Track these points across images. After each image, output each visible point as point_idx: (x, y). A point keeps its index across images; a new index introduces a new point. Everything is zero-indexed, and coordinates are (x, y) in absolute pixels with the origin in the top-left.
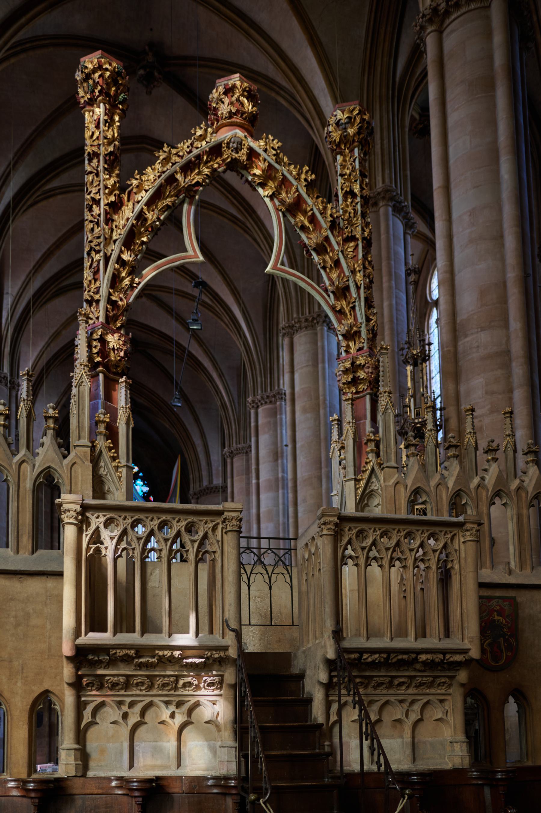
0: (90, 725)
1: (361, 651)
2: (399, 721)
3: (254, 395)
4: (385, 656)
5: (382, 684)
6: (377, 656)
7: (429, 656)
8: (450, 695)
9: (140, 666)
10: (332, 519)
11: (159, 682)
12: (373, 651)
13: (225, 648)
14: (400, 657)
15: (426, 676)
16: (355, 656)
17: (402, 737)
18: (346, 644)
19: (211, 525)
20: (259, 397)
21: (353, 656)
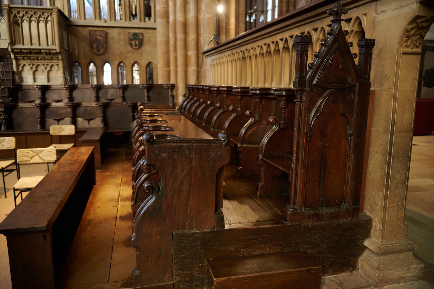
1: (21, 49)
2: (43, 70)
6: (26, 50)
7: (44, 51)
8: (59, 63)
10: (6, 8)
12: (25, 49)
14: (34, 51)
15: (49, 57)
16: (20, 50)
17: (45, 75)
18: (15, 47)
21: (18, 50)
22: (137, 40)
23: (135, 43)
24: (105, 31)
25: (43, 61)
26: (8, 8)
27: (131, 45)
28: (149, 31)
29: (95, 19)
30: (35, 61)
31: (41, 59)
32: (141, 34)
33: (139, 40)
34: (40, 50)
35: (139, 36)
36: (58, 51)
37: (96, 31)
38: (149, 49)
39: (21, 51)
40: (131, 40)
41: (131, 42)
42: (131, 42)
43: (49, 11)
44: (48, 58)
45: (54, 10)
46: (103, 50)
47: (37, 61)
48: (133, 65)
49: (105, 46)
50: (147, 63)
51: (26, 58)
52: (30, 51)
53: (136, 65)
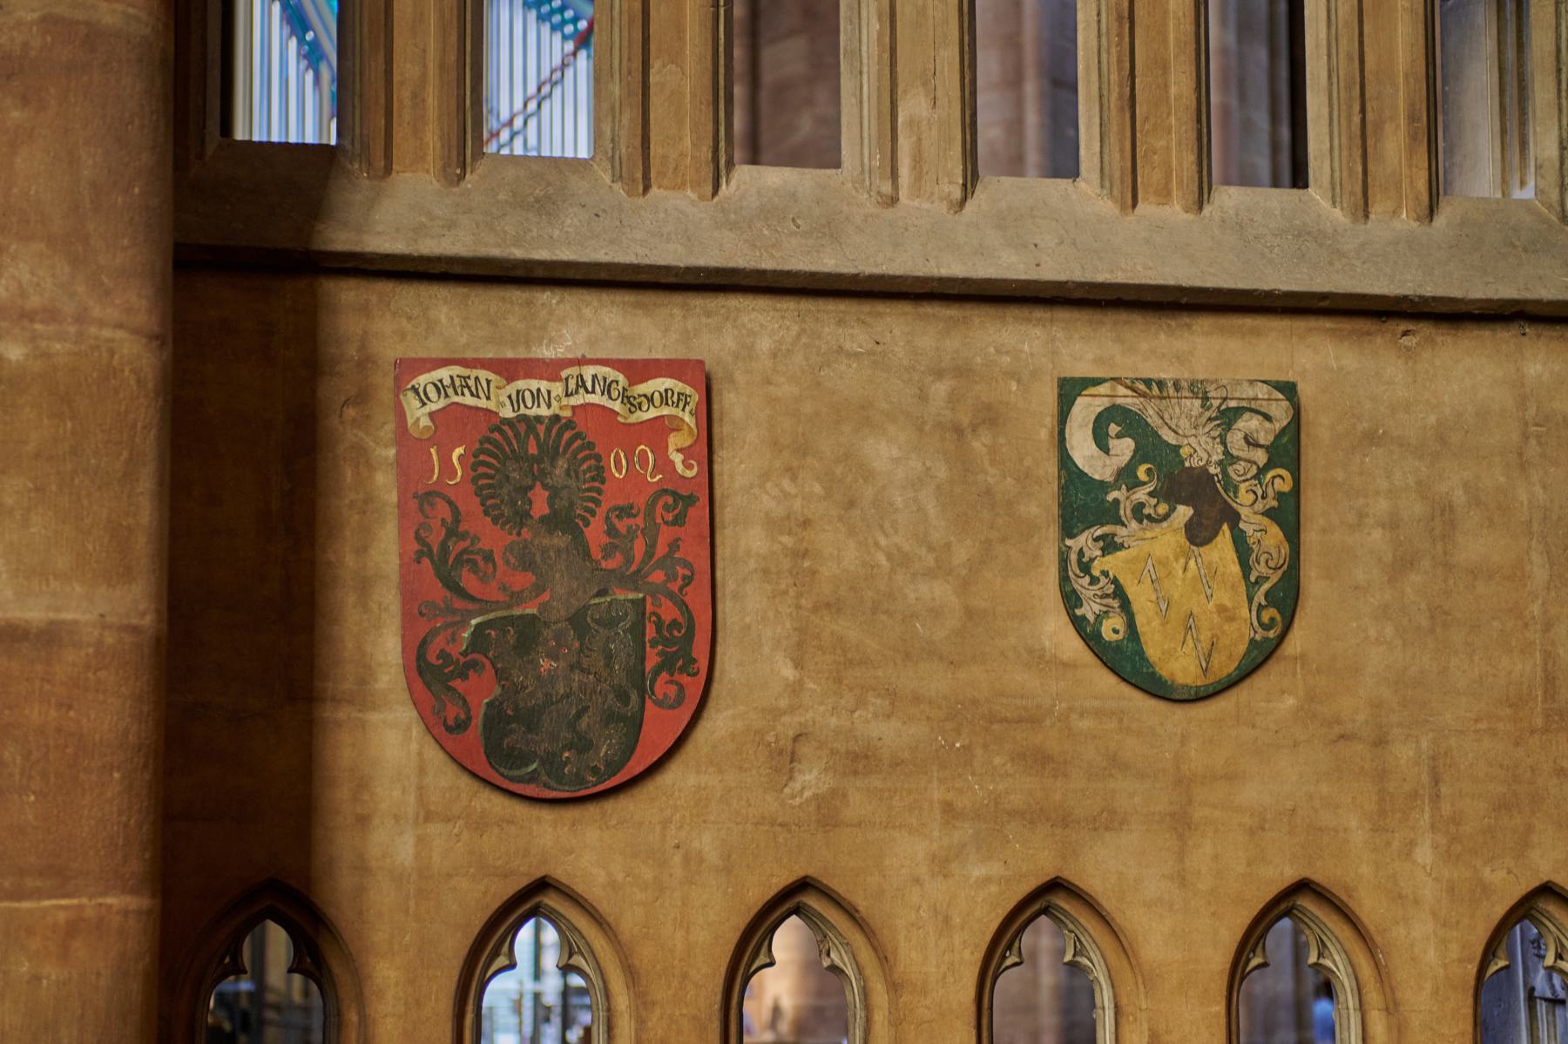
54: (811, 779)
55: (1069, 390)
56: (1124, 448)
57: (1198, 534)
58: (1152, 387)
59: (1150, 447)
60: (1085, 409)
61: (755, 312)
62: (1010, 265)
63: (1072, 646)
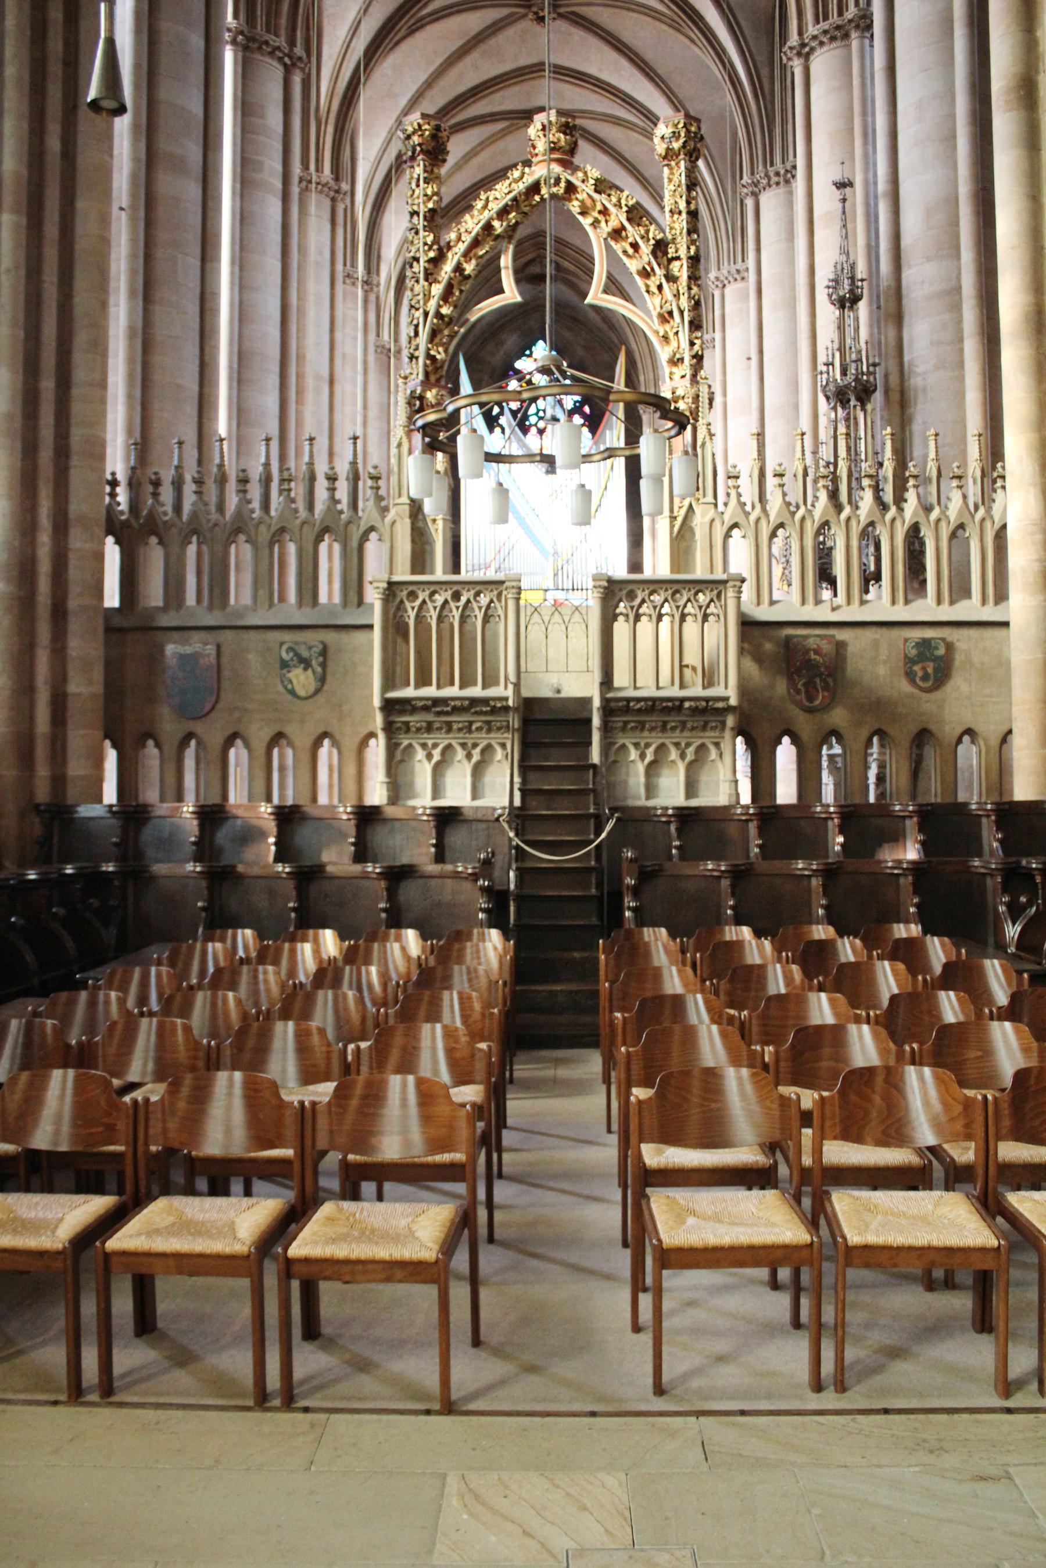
0: (402, 761)
1: (628, 700)
3: (719, 269)
4: (650, 703)
5: (656, 728)
6: (642, 703)
7: (692, 703)
9: (439, 714)
11: (455, 726)
12: (639, 700)
13: (506, 699)
14: (664, 704)
19: (495, 593)
20: (725, 272)
21: (621, 704)
22: (929, 660)
23: (924, 669)
24: (833, 636)
25: (677, 733)
26: (605, 584)
27: (910, 676)
28: (965, 632)
29: (803, 602)
30: (654, 734)
31: (673, 729)
32: (943, 640)
33: (937, 659)
34: (683, 700)
35: (937, 648)
36: (733, 702)
37: (806, 637)
38: (964, 688)
39: (628, 706)
40: (910, 661)
41: (910, 668)
42: (910, 668)
43: (715, 586)
44: (695, 724)
45: (730, 584)
46: (826, 694)
47: (660, 735)
48: (959, 741)
49: (830, 680)
50: (959, 730)
51: (633, 724)
52: (653, 706)
53: (966, 739)
54: (237, 714)
55: (282, 644)
56: (291, 654)
57: (305, 669)
58: (297, 643)
59: (297, 654)
60: (285, 647)
61: (228, 632)
62: (272, 622)
63: (281, 689)
